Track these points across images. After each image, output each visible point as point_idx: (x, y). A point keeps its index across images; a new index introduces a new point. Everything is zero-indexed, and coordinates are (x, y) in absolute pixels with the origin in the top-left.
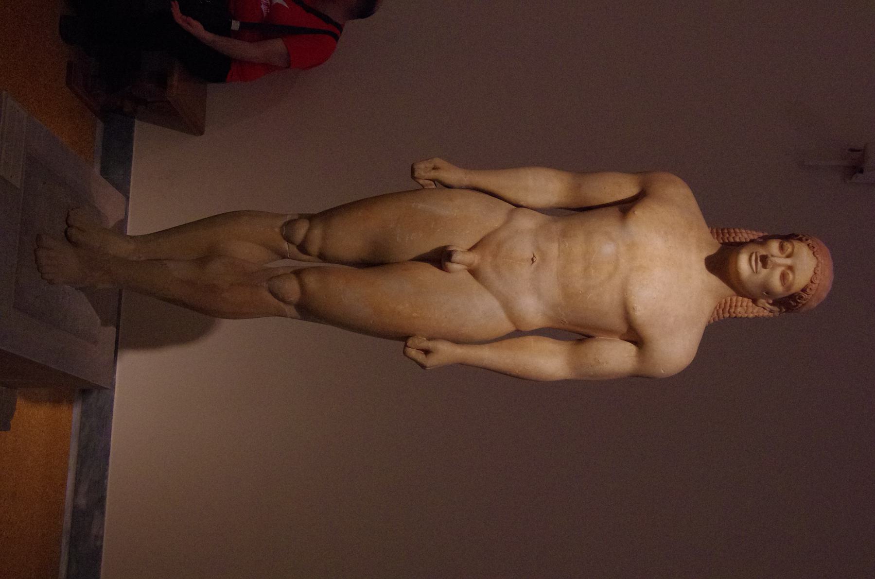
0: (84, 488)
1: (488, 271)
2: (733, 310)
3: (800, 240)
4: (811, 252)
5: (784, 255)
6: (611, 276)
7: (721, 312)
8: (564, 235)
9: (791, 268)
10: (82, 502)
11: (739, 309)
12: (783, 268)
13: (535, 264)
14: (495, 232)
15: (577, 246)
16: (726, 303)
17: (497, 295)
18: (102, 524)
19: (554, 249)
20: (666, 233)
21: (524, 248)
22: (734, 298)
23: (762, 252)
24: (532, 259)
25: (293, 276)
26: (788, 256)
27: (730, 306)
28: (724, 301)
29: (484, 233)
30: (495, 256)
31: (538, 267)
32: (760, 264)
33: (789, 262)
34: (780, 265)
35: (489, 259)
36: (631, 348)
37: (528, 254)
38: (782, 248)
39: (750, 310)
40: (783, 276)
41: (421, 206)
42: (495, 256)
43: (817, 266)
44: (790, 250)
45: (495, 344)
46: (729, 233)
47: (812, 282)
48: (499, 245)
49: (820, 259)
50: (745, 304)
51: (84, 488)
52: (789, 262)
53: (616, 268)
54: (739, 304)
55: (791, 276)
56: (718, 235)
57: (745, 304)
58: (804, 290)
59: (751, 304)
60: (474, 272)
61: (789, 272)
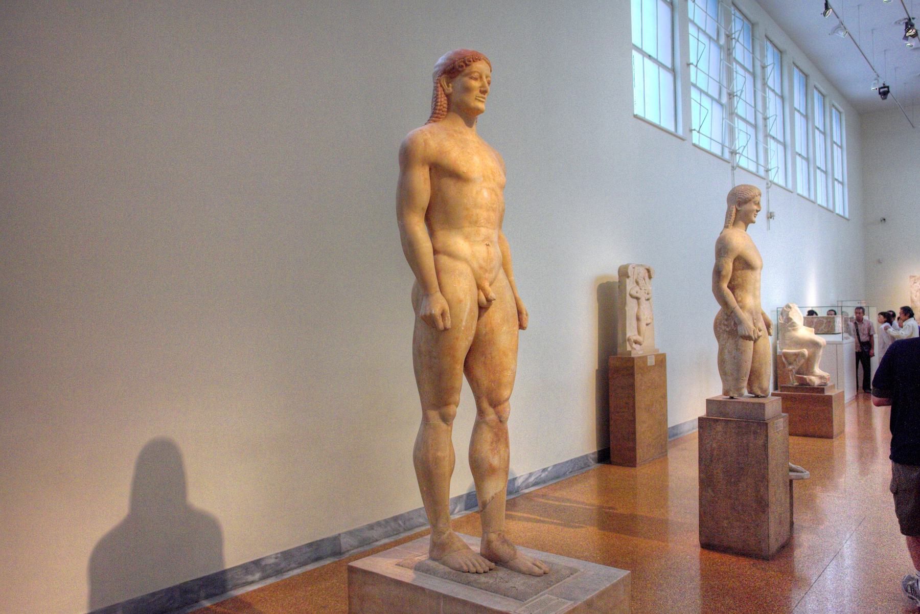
0: (250, 578)
1: (490, 276)
3: (467, 65)
6: (496, 195)
8: (475, 223)
10: (257, 576)
14: (473, 271)
15: (483, 214)
18: (269, 557)
19: (483, 230)
21: (481, 250)
23: (477, 93)
25: (500, 408)
26: (481, 77)
30: (486, 271)
37: (484, 248)
38: (476, 79)
41: (464, 324)
42: (486, 271)
48: (481, 268)
51: (250, 578)
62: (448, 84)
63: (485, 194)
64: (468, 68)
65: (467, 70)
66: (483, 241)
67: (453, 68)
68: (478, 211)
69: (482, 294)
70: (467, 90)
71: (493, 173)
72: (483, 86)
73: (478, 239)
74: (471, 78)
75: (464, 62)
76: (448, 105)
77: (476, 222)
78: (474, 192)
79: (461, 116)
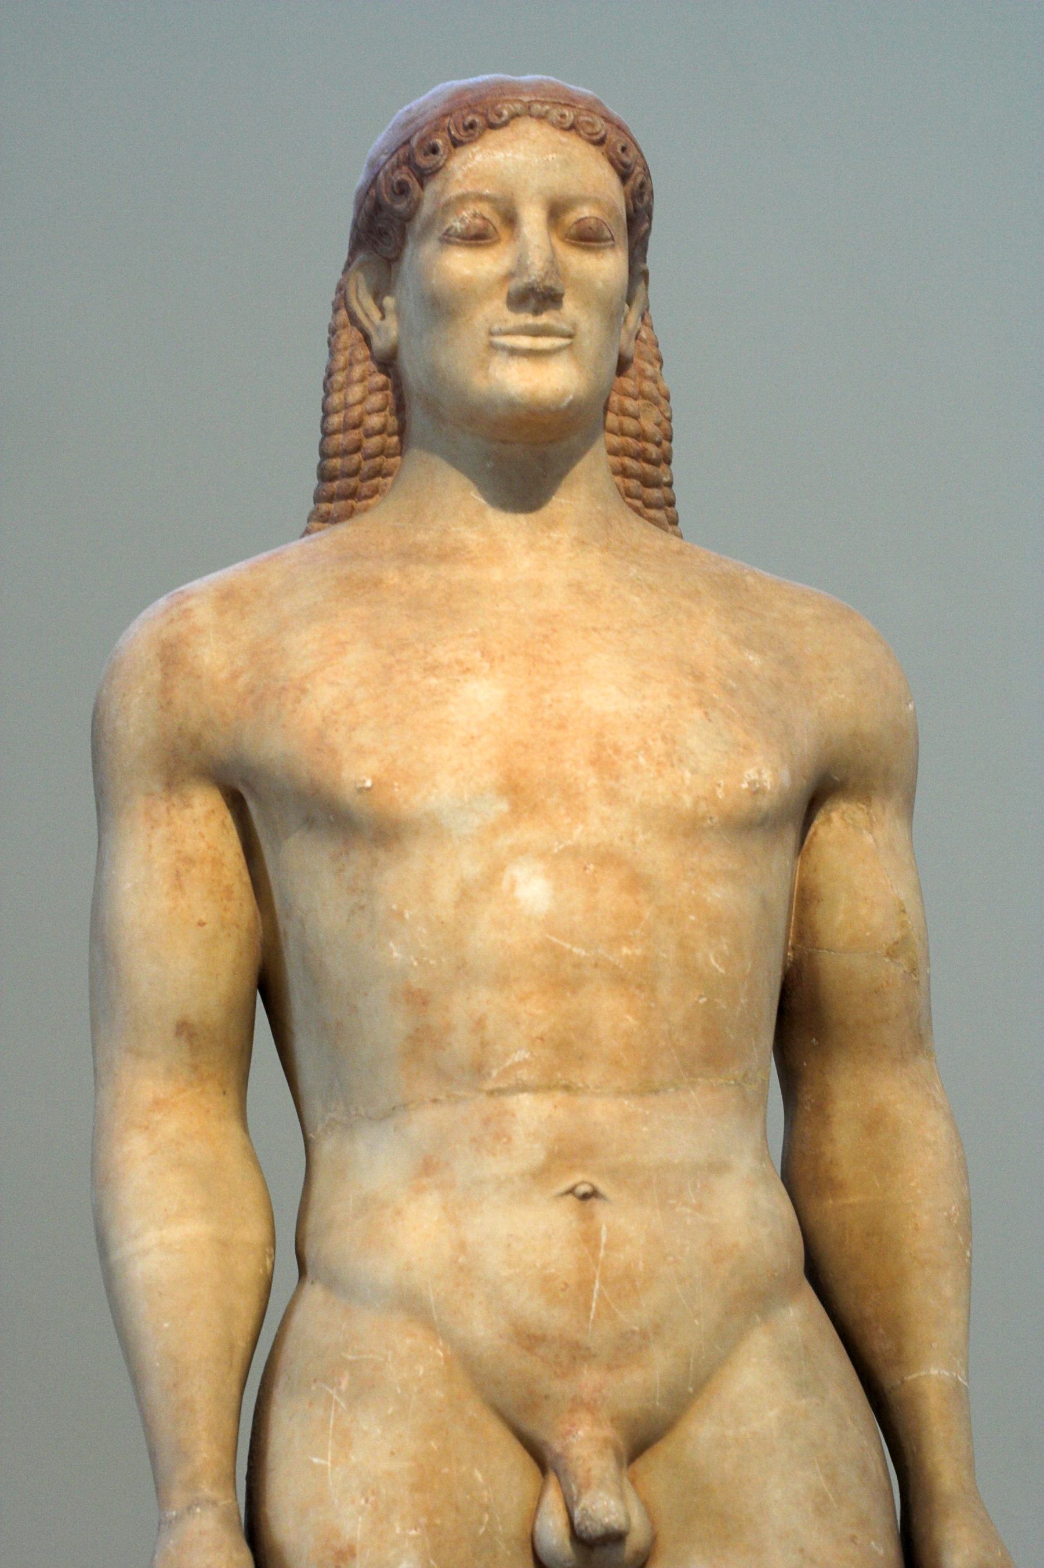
2: (653, 451)
3: (424, 176)
4: (493, 137)
5: (504, 233)
7: (655, 494)
9: (556, 211)
11: (649, 427)
13: (602, 1187)
16: (623, 472)
17: (726, 1341)
20: (432, 669)
22: (616, 440)
24: (585, 1197)
26: (511, 220)
27: (640, 456)
28: (618, 479)
29: (473, 1408)
31: (622, 1175)
32: (544, 319)
33: (533, 220)
35: (589, 1378)
36: (836, 823)
39: (648, 386)
40: (587, 238)
42: (578, 1354)
43: (541, 117)
44: (485, 209)
45: (878, 1345)
46: (346, 453)
47: (600, 142)
48: (529, 1339)
49: (518, 107)
50: (630, 404)
52: (533, 220)
53: (607, 858)
54: (630, 424)
55: (585, 211)
56: (353, 494)
57: (630, 404)
58: (624, 176)
59: (628, 384)
60: (640, 1442)
61: (571, 218)
62: (377, 297)
63: (533, 890)
64: (434, 187)
65: (430, 196)
66: (541, 1175)
67: (378, 207)
68: (483, 1000)
69: (553, 1498)
70: (443, 308)
71: (604, 760)
72: (521, 266)
73: (496, 1166)
74: (449, 239)
75: (409, 161)
76: (400, 408)
77: (479, 1069)
78: (445, 892)
79: (454, 461)
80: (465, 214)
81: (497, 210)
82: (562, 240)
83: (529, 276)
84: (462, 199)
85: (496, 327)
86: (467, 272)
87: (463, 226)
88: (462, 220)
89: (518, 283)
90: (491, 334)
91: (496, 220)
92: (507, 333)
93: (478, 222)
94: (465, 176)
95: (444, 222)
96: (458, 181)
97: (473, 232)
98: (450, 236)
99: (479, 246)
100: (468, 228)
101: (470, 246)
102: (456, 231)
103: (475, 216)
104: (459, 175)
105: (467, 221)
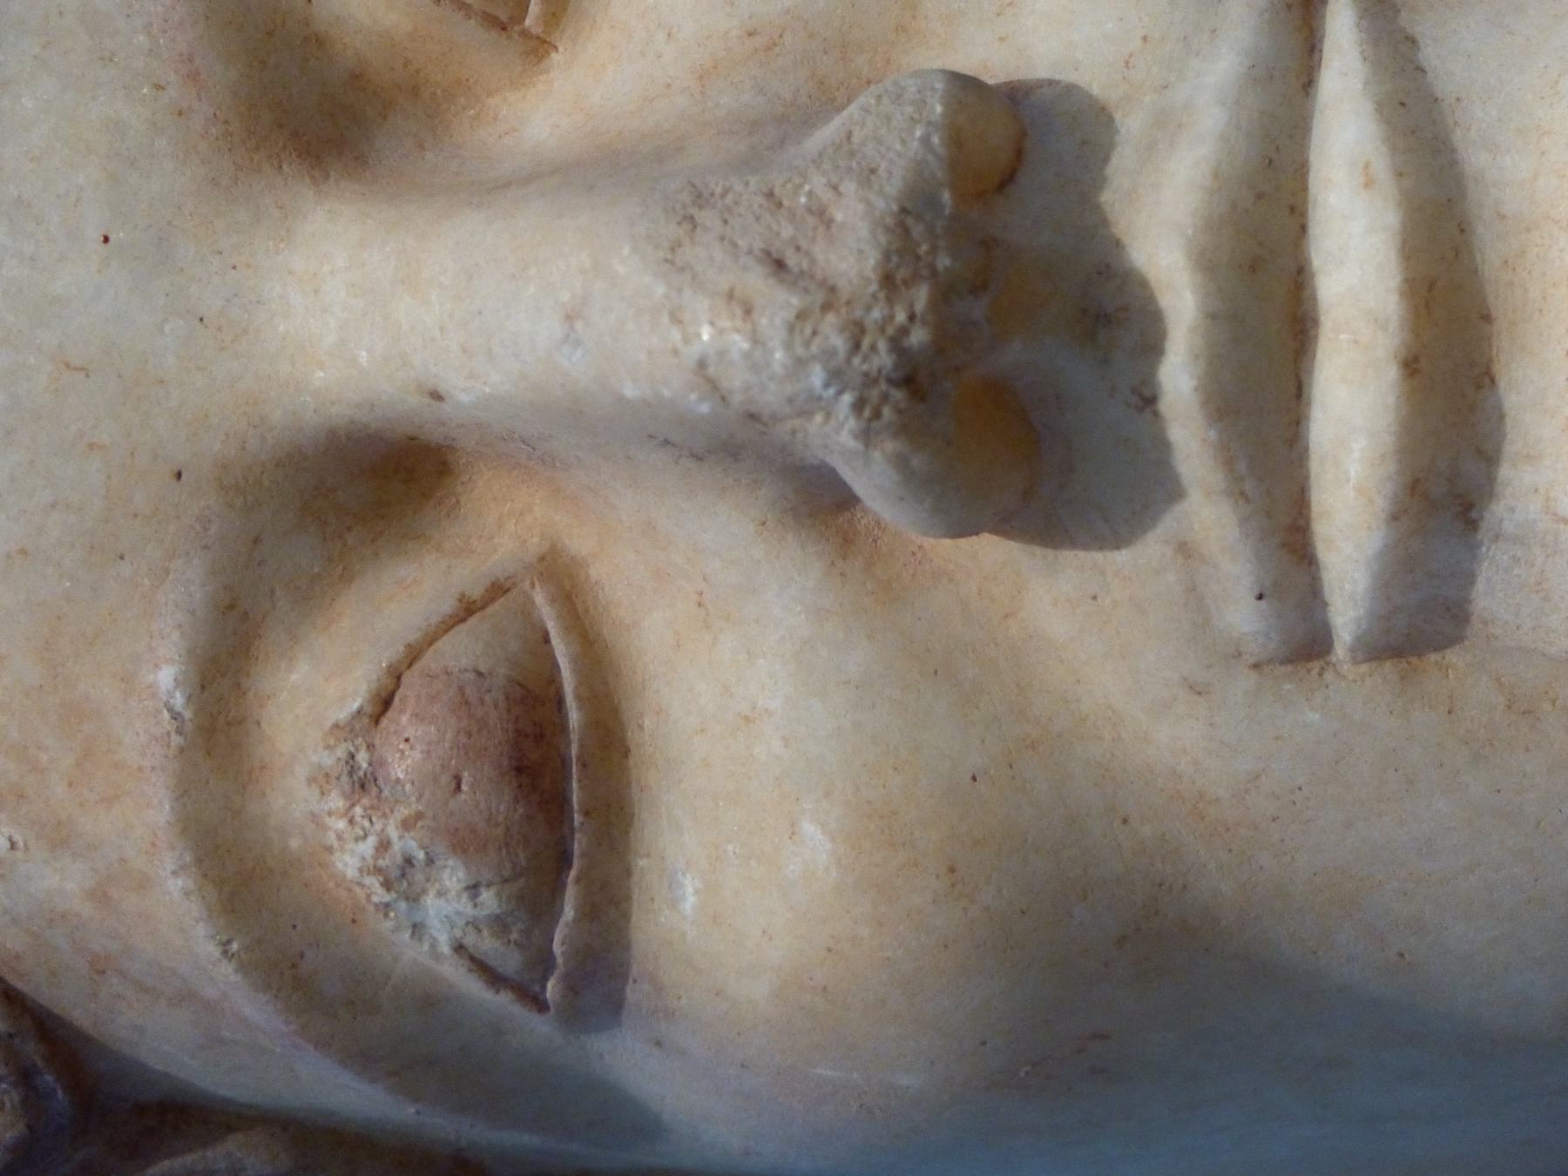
5: (498, 527)
12: (546, 110)
26: (381, 478)
32: (1162, 232)
33: (364, 304)
34: (605, 169)
38: (552, 771)
44: (312, 691)
52: (364, 304)
72: (735, 446)
80: (350, 860)
81: (313, 594)
82: (539, 48)
83: (808, 406)
84: (241, 873)
85: (1242, 616)
86: (813, 847)
87: (453, 875)
88: (402, 878)
89: (873, 479)
90: (1308, 646)
91: (397, 601)
92: (1289, 537)
93: (410, 751)
94: (60, 838)
95: (430, 1001)
96: (100, 896)
97: (485, 798)
98: (543, 962)
99: (611, 738)
100: (464, 842)
101: (615, 817)
102: (500, 924)
103: (363, 784)
104: (60, 882)
105: (406, 843)
